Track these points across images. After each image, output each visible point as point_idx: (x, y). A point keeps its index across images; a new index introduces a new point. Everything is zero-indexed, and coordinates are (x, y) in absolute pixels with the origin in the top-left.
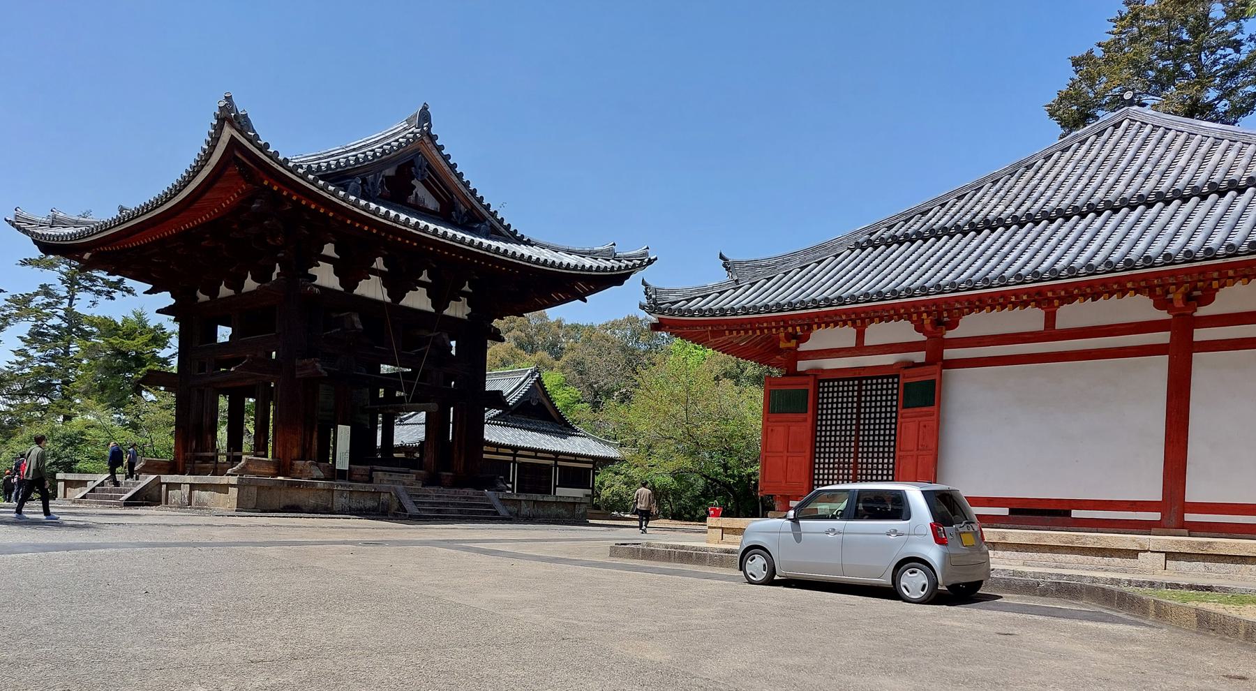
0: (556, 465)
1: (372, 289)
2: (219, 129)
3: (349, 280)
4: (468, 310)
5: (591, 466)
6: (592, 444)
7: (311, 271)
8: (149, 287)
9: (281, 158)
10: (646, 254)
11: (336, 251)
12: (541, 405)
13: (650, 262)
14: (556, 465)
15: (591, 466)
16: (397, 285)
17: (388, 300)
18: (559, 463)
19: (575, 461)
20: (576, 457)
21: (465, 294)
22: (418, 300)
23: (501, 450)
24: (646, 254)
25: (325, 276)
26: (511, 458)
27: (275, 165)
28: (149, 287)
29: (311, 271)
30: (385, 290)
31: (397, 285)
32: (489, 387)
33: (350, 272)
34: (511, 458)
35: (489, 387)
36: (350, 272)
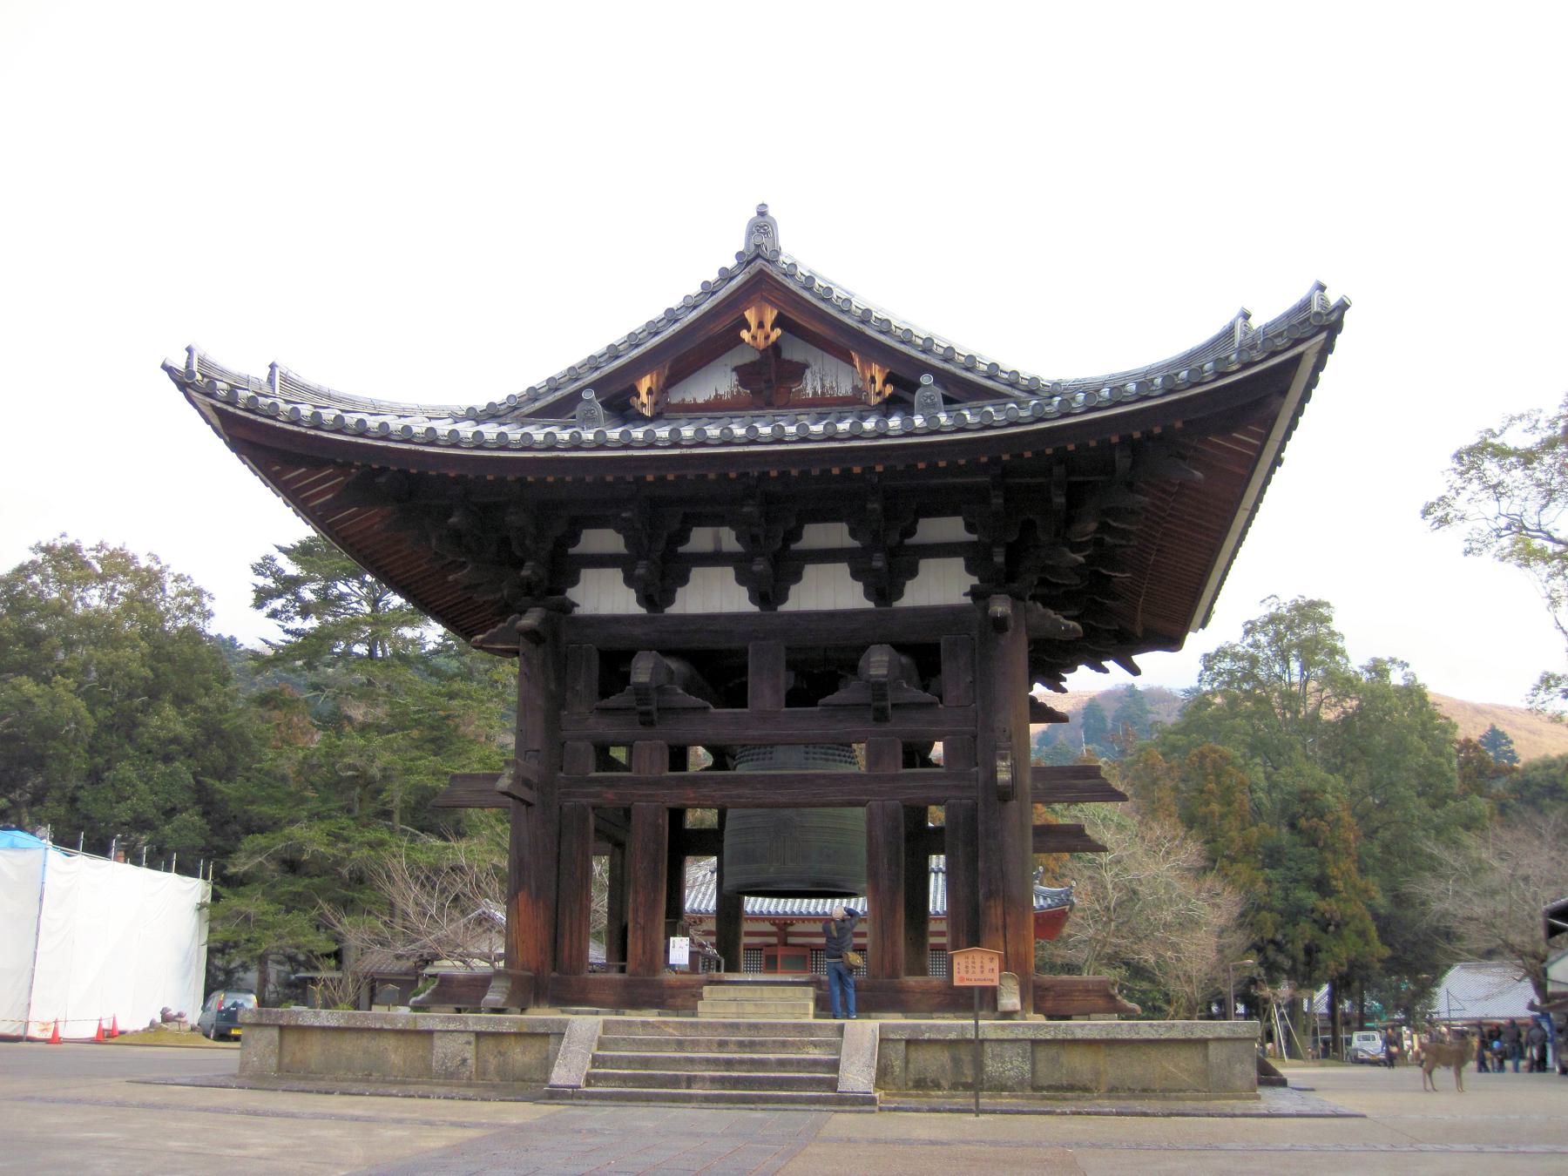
3: (656, 593)
16: (771, 572)
25: (605, 596)
31: (771, 572)
33: (658, 574)
36: (658, 574)
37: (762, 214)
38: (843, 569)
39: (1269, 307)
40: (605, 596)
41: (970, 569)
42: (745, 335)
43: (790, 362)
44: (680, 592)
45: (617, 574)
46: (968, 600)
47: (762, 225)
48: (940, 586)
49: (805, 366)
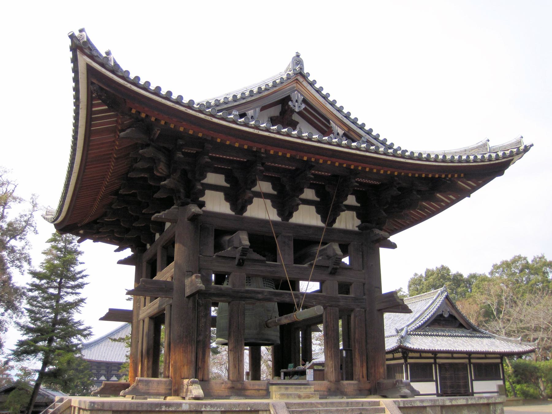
0: (470, 363)
1: (261, 210)
2: (75, 60)
4: (358, 222)
5: (498, 361)
6: (497, 342)
7: (201, 199)
8: (117, 247)
9: (142, 82)
10: (519, 142)
11: (226, 181)
12: (452, 317)
13: (526, 149)
14: (470, 363)
15: (498, 361)
16: (285, 203)
17: (278, 219)
18: (473, 361)
19: (486, 358)
20: (486, 355)
21: (350, 208)
22: (307, 217)
23: (424, 355)
24: (519, 142)
25: (216, 204)
26: (432, 361)
27: (129, 85)
28: (117, 247)
29: (201, 199)
30: (275, 211)
31: (285, 203)
32: (386, 289)
33: (238, 197)
34: (432, 361)
35: (386, 289)
37: (298, 56)
38: (313, 208)
39: (499, 140)
40: (216, 204)
41: (358, 217)
42: (290, 103)
43: (294, 121)
44: (249, 207)
45: (221, 195)
46: (357, 229)
47: (298, 60)
48: (347, 221)
49: (298, 123)
